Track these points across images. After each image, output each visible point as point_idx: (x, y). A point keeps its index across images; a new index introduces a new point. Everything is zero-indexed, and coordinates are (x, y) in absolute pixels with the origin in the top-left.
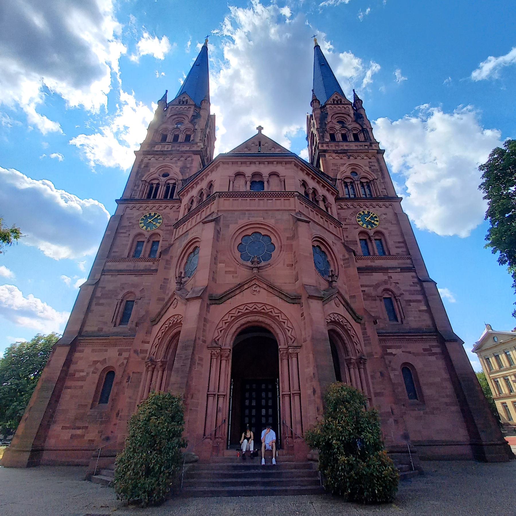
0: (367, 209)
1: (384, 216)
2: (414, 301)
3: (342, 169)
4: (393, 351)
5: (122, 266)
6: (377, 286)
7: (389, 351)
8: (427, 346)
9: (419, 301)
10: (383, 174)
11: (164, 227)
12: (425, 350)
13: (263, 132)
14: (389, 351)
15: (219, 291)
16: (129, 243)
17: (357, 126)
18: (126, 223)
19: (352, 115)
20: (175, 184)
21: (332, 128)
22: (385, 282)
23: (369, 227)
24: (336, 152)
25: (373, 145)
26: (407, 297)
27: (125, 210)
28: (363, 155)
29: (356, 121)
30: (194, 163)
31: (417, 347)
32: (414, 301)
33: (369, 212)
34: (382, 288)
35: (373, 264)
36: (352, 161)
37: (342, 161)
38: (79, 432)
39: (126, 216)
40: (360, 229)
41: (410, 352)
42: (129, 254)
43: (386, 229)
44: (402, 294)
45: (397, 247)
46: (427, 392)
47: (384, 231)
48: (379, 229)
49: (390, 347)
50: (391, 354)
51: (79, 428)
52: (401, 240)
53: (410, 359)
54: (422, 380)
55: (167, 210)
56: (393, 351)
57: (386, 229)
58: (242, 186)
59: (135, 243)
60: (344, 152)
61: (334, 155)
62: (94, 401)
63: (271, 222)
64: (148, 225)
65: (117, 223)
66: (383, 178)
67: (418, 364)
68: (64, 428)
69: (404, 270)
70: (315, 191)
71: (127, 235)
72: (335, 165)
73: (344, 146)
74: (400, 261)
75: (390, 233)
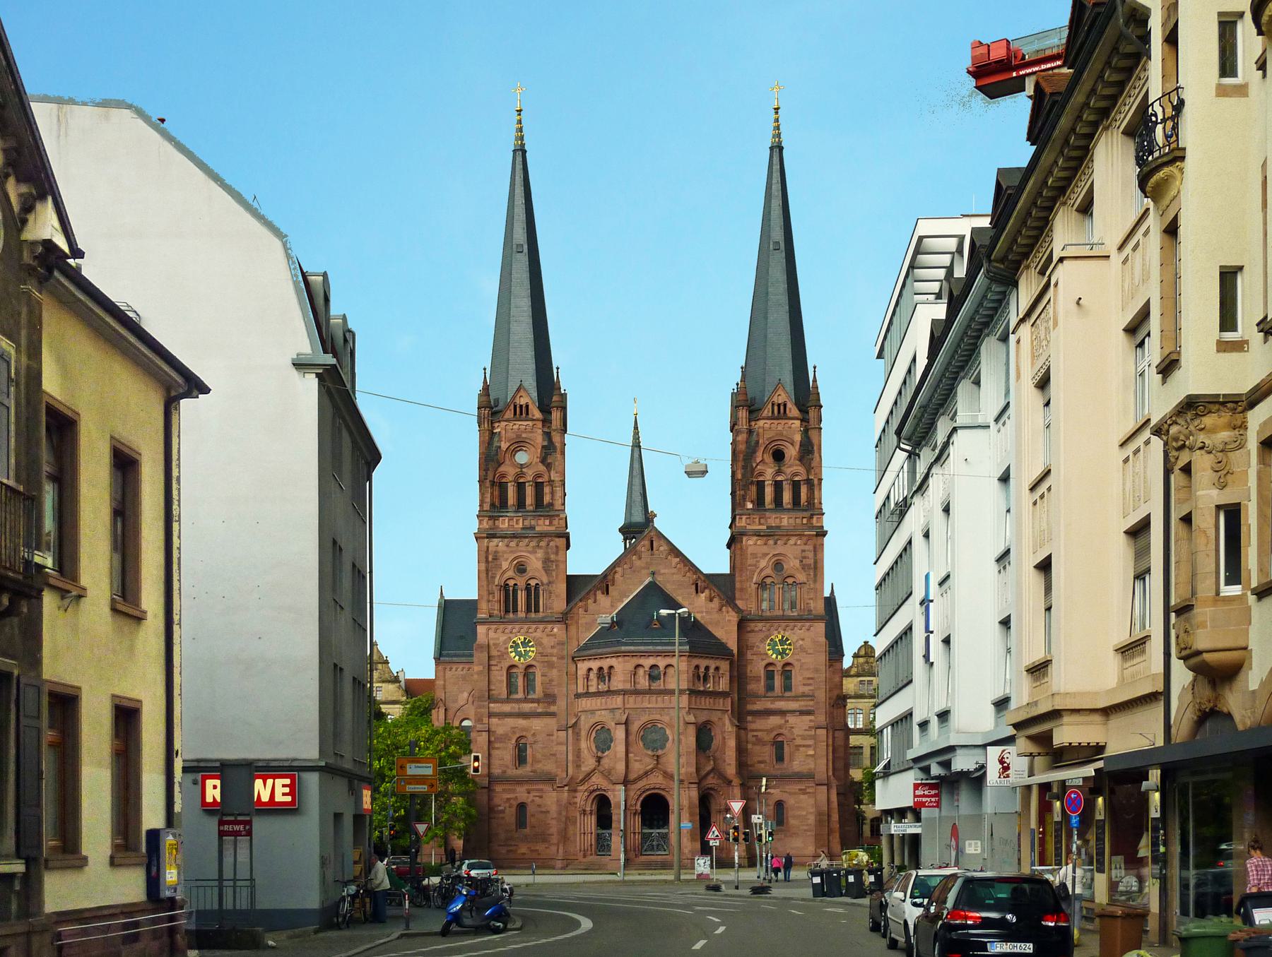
3: (763, 563)
5: (507, 708)
6: (772, 730)
9: (809, 746)
10: (815, 575)
11: (539, 658)
15: (632, 776)
17: (801, 469)
19: (797, 447)
22: (780, 727)
24: (758, 534)
26: (799, 741)
31: (796, 787)
37: (765, 549)
46: (792, 822)
47: (795, 663)
53: (784, 797)
54: (790, 813)
55: (538, 634)
60: (771, 534)
66: (815, 581)
67: (790, 801)
69: (802, 713)
72: (754, 555)
73: (773, 519)
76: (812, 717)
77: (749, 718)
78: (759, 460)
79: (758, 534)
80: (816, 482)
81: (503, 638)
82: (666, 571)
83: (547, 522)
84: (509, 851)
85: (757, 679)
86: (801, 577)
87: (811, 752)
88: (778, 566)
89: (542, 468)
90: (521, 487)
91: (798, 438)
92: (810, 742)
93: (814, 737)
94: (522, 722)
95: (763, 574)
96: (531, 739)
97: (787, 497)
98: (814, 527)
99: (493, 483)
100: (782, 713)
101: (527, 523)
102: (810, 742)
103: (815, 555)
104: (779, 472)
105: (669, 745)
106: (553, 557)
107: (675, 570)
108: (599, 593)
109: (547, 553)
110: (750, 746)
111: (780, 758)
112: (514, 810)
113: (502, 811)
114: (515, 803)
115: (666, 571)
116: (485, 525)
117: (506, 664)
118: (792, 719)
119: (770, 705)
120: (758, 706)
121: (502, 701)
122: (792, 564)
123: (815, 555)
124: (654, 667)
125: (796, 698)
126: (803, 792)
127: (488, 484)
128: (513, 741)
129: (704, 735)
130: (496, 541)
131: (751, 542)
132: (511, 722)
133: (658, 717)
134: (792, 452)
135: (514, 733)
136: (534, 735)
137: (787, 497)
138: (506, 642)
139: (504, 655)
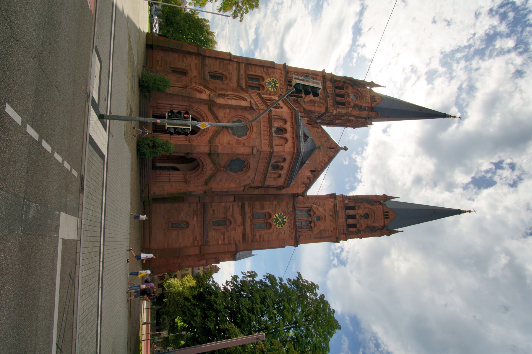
0: (287, 221)
1: (283, 232)
2: (224, 238)
3: (321, 209)
4: (195, 219)
5: (242, 72)
6: (233, 217)
7: (195, 216)
8: (198, 239)
9: (224, 241)
12: (196, 237)
13: (342, 152)
14: (195, 216)
16: (257, 74)
17: (363, 227)
18: (270, 71)
19: (373, 225)
20: (302, 97)
21: (359, 207)
22: (235, 223)
23: (274, 220)
24: (335, 206)
25: (344, 236)
26: (227, 234)
27: (279, 69)
28: (334, 226)
29: (368, 227)
30: (319, 108)
32: (224, 238)
33: (285, 222)
34: (232, 220)
35: (247, 217)
36: (328, 218)
38: (160, 63)
39: (275, 70)
40: (272, 214)
41: (195, 228)
42: (250, 75)
43: (273, 231)
44: (228, 231)
45: (260, 236)
48: (273, 226)
49: (197, 217)
50: (194, 217)
51: (161, 63)
52: (265, 239)
56: (195, 219)
57: (273, 231)
58: (277, 124)
59: (258, 77)
60: (335, 212)
61: (333, 205)
62: (173, 68)
63: (254, 136)
64: (270, 83)
65: (270, 65)
66: (315, 238)
68: (162, 56)
69: (244, 236)
70: (282, 168)
71: (262, 72)
73: (342, 214)
74: (250, 235)
75: (270, 233)
76: (241, 241)
77: (240, 204)
78: (366, 205)
79: (335, 206)
80: (359, 235)
81: (277, 76)
82: (321, 155)
83: (331, 104)
84: (158, 61)
85: (262, 208)
86: (316, 230)
87: (220, 242)
88: (319, 218)
89: (352, 105)
90: (343, 96)
91: (376, 225)
92: (226, 242)
93: (230, 243)
94: (235, 78)
95: (315, 210)
96: (226, 82)
97: (351, 221)
98: (340, 235)
99: (344, 82)
100: (244, 223)
101: (330, 95)
102: (226, 242)
103: (327, 237)
104: (361, 216)
105: (236, 137)
106: (316, 105)
107: (321, 159)
108: (308, 119)
109: (318, 102)
110: (223, 204)
111: (217, 223)
112: (184, 67)
113: (183, 61)
114: (188, 69)
115: (321, 155)
116: (327, 76)
117: (264, 76)
118: (240, 230)
119: (248, 216)
120: (247, 209)
121: (246, 71)
122: (321, 225)
123: (327, 237)
124: (285, 131)
125: (252, 231)
126: (195, 239)
127: (344, 80)
128: (224, 73)
129: (239, 164)
130: (322, 79)
131: (330, 202)
132: (235, 73)
133: (255, 130)
134: (370, 222)
135: (229, 74)
136: (228, 84)
137: (351, 221)
138: (275, 77)
139: (269, 75)
